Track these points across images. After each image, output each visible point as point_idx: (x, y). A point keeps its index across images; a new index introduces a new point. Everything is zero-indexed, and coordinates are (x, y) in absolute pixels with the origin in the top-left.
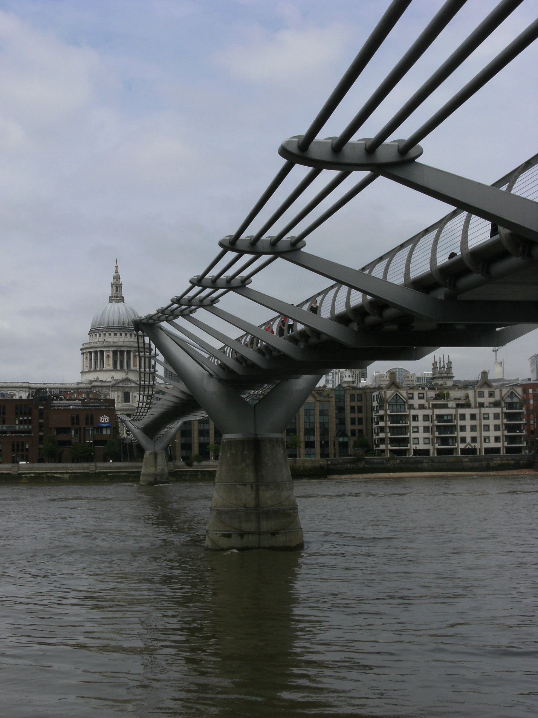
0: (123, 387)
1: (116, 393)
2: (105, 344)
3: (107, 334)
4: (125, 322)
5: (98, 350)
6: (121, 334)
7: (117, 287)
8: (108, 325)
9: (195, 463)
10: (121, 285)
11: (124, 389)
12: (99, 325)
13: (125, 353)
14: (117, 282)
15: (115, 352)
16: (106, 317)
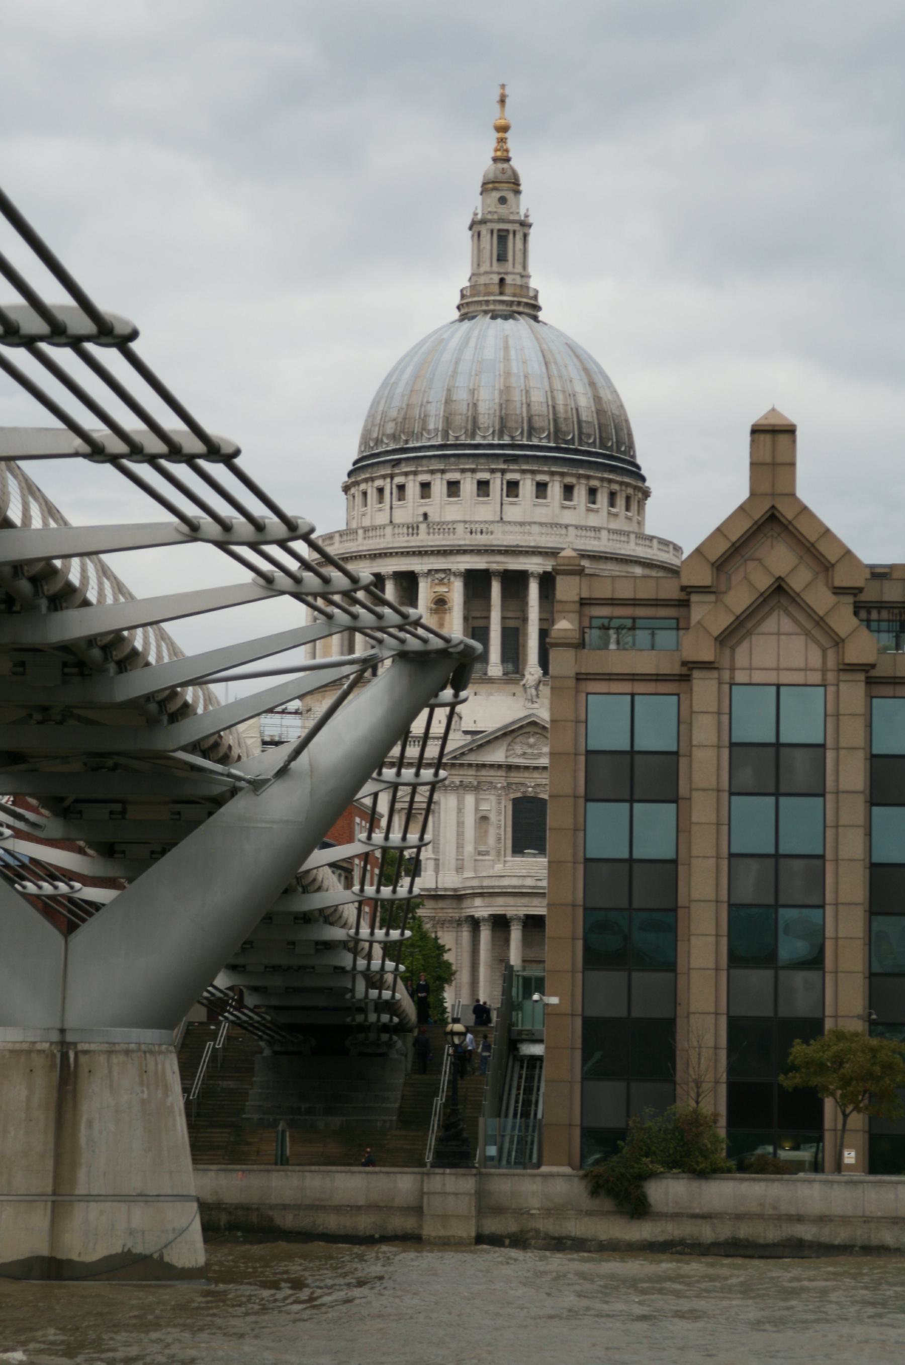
0: (510, 768)
1: (470, 799)
2: (424, 539)
3: (439, 487)
4: (538, 423)
5: (388, 567)
6: (512, 488)
7: (502, 237)
8: (446, 434)
9: (668, 1191)
10: (525, 224)
11: (516, 777)
12: (394, 437)
13: (534, 589)
14: (502, 210)
15: (477, 582)
16: (436, 397)
